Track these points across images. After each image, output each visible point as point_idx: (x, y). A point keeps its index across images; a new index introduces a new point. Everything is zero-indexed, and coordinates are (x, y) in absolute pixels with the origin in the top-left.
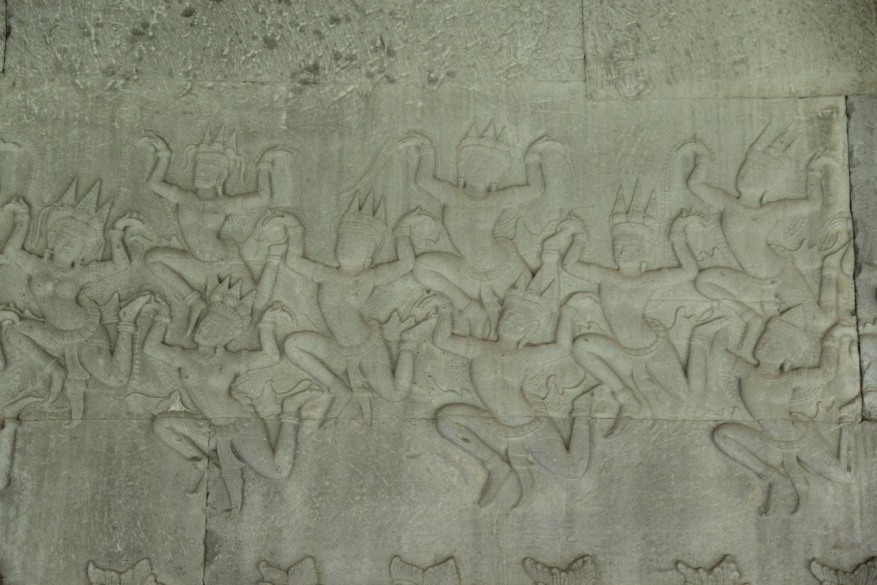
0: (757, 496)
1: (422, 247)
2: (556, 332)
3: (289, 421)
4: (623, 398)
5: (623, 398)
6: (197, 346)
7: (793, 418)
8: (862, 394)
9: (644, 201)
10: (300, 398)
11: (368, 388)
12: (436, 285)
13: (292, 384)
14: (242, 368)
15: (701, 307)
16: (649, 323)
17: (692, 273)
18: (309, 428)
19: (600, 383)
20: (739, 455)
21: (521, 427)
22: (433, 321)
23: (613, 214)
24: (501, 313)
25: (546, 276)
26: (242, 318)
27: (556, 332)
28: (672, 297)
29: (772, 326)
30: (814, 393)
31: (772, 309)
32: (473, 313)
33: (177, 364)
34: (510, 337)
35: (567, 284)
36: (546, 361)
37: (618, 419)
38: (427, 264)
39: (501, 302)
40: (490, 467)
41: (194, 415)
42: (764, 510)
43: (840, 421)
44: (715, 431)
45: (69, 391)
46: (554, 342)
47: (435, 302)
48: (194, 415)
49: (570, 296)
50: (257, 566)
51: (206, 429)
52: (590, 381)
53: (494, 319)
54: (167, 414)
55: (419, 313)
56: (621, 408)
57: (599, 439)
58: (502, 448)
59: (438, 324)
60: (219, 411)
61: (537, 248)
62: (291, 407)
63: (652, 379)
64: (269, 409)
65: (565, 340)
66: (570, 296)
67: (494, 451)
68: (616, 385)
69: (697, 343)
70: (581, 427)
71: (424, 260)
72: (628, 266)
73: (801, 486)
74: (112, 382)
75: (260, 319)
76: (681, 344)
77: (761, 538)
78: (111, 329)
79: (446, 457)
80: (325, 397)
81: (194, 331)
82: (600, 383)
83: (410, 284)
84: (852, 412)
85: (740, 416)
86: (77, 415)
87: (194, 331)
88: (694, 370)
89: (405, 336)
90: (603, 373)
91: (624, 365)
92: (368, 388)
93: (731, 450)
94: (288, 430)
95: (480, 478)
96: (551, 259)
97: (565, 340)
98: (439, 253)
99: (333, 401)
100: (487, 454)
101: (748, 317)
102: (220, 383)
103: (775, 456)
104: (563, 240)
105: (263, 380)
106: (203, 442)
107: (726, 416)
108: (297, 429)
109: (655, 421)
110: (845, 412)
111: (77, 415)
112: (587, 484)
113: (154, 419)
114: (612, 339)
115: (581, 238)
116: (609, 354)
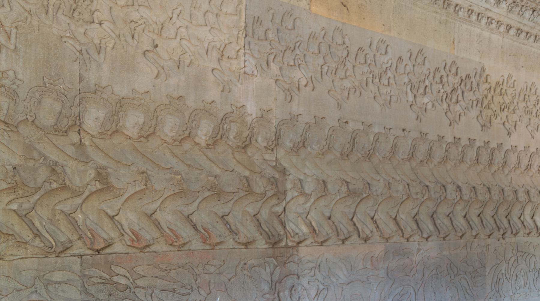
0: (221, 88)
1: (140, 3)
2: (176, 36)
3: (103, 46)
4: (192, 57)
5: (192, 57)
6: (74, 17)
7: (230, 70)
8: (245, 67)
9: (199, 5)
10: (106, 40)
11: (126, 41)
12: (144, 15)
13: (103, 36)
14: (88, 28)
15: (211, 37)
16: (199, 39)
17: (209, 28)
18: (109, 49)
19: (186, 52)
20: (218, 77)
21: (167, 60)
22: (144, 26)
23: (191, 7)
24: (162, 28)
25: (174, 19)
26: (87, 12)
27: (176, 36)
28: (203, 33)
29: (227, 46)
30: (235, 65)
31: (227, 42)
32: (154, 26)
33: (68, 21)
34: (164, 35)
35: (179, 24)
36: (174, 43)
37: (190, 63)
38: (142, 9)
39: (162, 25)
40: (159, 69)
41: (74, 38)
42: (223, 91)
43: (240, 72)
44: (213, 70)
45: (33, 22)
46: (176, 39)
47: (144, 20)
48: (74, 38)
49: (180, 27)
50: (95, 86)
51: (78, 43)
52: (184, 52)
53: (160, 29)
54: (65, 36)
55: (140, 23)
56: (191, 60)
57: (186, 67)
58: (162, 65)
59: (145, 27)
60: (82, 39)
61: (171, 11)
62: (103, 42)
63: (199, 54)
64: (97, 41)
65: (178, 39)
66: (180, 27)
67: (160, 66)
68: (191, 54)
69: (210, 46)
70: (182, 63)
71: (141, 7)
72: (194, 22)
73: (231, 87)
74: (47, 22)
75: (93, 14)
76: (206, 46)
77: (221, 98)
78: (46, 6)
79: (147, 65)
80: (113, 41)
81: (73, 13)
82: (186, 52)
83: (137, 13)
84: (242, 71)
85: (219, 67)
86: (36, 31)
87: (73, 13)
88: (209, 53)
89: (136, 28)
90: (187, 50)
91: (192, 49)
92: (126, 41)
93: (217, 75)
94: (103, 49)
95: (156, 72)
96: (175, 16)
97: (178, 39)
98: (145, 6)
99: (115, 43)
100: (158, 66)
101: (221, 43)
102: (82, 30)
103: (226, 79)
104: (178, 11)
105: (95, 33)
106: (77, 47)
107: (215, 67)
108: (105, 49)
109: (199, 65)
110: (241, 71)
111: (36, 31)
112: (183, 78)
113: (61, 37)
114: (190, 41)
115: (183, 11)
116: (189, 45)
